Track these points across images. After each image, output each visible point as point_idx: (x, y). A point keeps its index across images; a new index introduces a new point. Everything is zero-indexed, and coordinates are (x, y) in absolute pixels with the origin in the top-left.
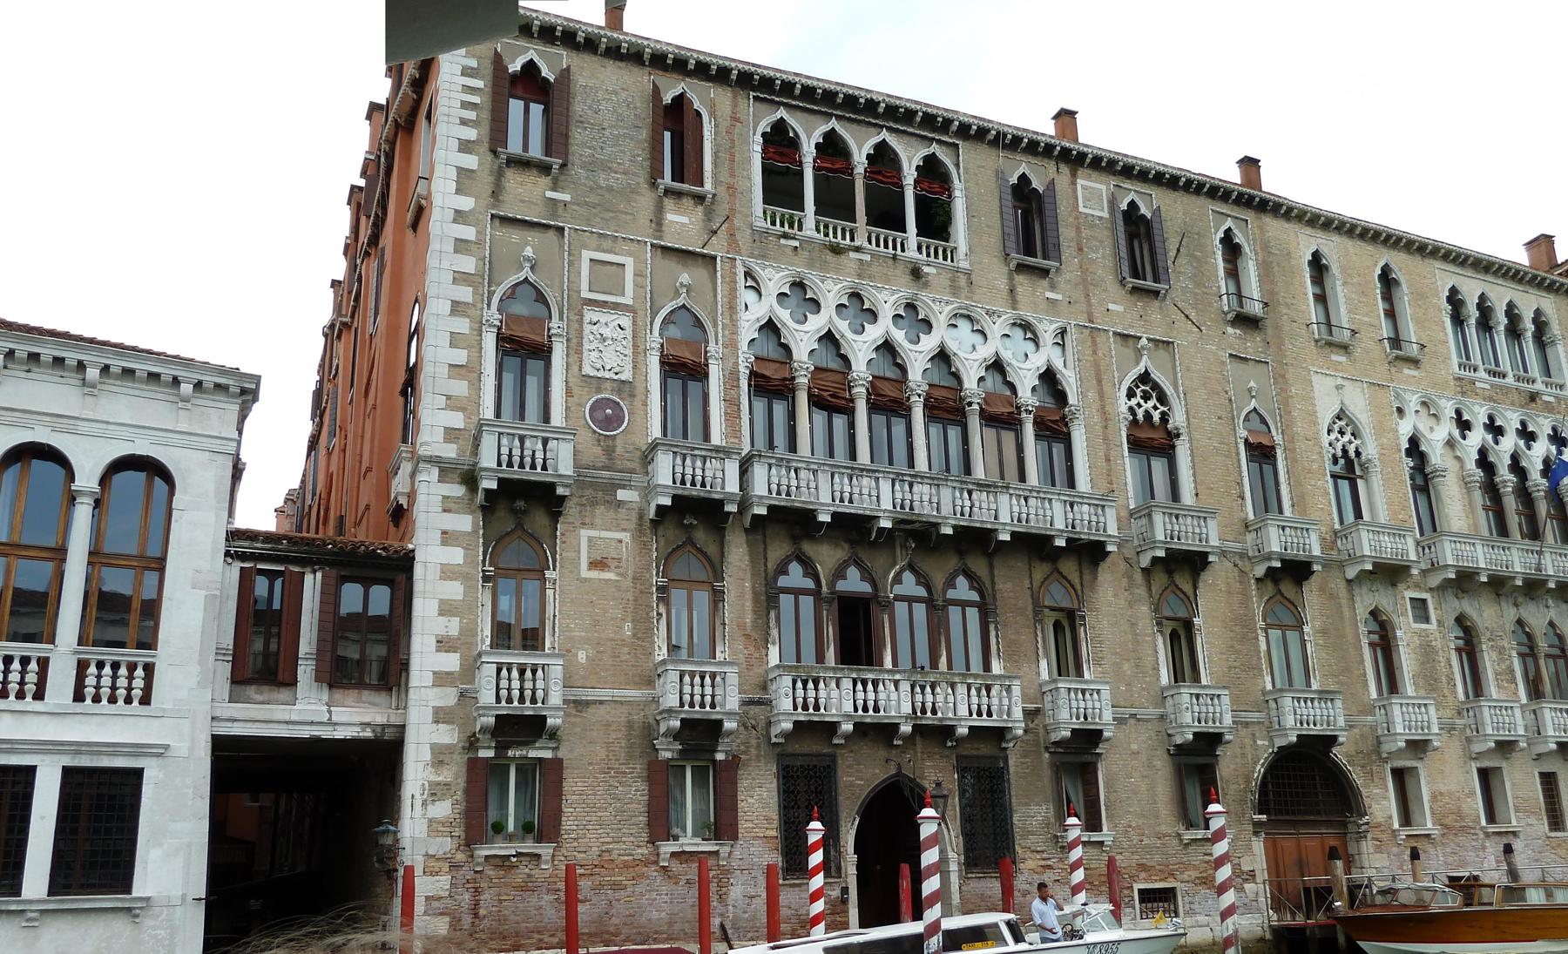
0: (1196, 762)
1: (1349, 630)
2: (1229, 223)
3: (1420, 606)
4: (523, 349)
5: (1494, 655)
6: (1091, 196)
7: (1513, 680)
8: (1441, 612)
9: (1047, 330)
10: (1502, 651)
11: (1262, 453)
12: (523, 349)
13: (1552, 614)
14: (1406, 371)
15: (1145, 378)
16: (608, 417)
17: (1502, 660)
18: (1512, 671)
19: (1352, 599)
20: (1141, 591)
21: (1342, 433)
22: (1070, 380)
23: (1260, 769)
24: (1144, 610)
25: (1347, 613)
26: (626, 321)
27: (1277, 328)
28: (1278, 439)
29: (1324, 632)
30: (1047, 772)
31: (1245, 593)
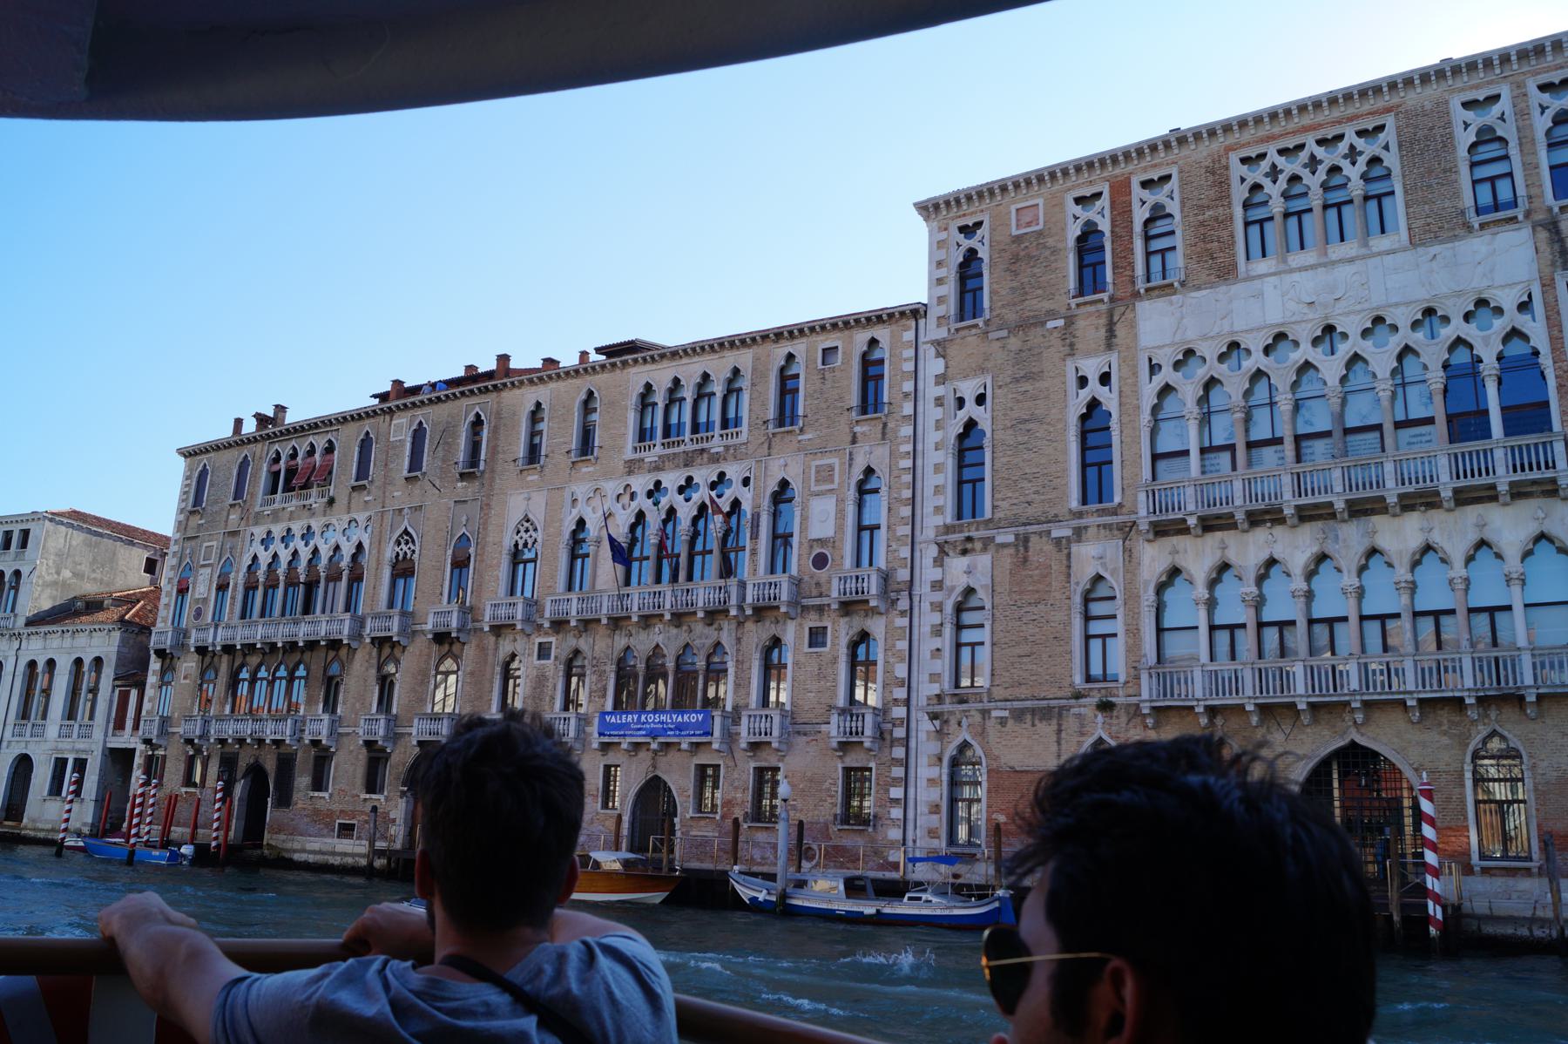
0: (376, 757)
1: (489, 669)
2: (477, 409)
3: (544, 651)
4: (182, 591)
5: (594, 678)
6: (400, 427)
7: (604, 696)
8: (560, 646)
9: (361, 517)
10: (601, 674)
11: (460, 564)
12: (182, 591)
13: (660, 639)
14: (584, 470)
15: (406, 532)
16: (198, 614)
17: (599, 681)
18: (605, 689)
19: (496, 649)
20: (375, 662)
21: (527, 531)
22: (366, 546)
23: (410, 760)
24: (373, 671)
25: (490, 658)
26: (209, 570)
27: (493, 471)
28: (472, 550)
29: (472, 674)
30: (311, 761)
31: (429, 656)
